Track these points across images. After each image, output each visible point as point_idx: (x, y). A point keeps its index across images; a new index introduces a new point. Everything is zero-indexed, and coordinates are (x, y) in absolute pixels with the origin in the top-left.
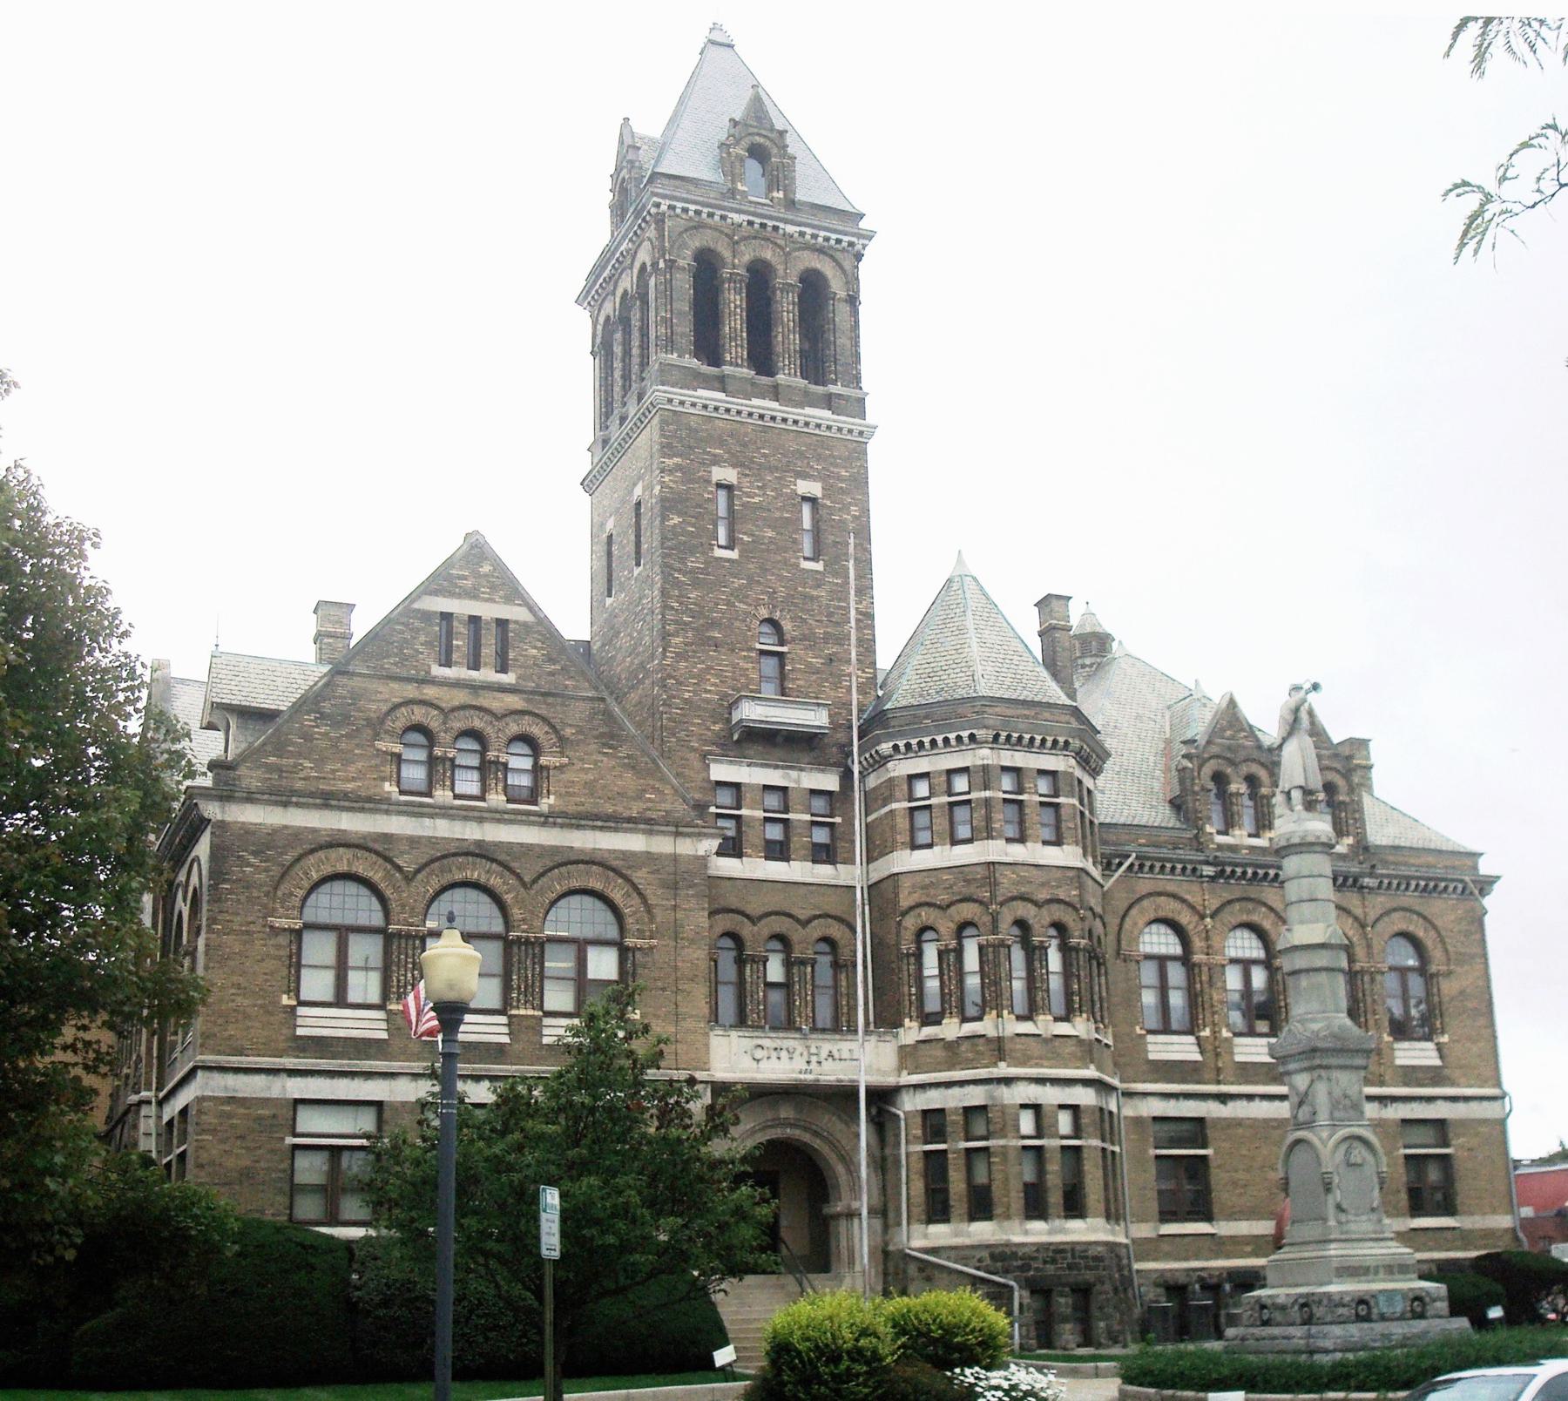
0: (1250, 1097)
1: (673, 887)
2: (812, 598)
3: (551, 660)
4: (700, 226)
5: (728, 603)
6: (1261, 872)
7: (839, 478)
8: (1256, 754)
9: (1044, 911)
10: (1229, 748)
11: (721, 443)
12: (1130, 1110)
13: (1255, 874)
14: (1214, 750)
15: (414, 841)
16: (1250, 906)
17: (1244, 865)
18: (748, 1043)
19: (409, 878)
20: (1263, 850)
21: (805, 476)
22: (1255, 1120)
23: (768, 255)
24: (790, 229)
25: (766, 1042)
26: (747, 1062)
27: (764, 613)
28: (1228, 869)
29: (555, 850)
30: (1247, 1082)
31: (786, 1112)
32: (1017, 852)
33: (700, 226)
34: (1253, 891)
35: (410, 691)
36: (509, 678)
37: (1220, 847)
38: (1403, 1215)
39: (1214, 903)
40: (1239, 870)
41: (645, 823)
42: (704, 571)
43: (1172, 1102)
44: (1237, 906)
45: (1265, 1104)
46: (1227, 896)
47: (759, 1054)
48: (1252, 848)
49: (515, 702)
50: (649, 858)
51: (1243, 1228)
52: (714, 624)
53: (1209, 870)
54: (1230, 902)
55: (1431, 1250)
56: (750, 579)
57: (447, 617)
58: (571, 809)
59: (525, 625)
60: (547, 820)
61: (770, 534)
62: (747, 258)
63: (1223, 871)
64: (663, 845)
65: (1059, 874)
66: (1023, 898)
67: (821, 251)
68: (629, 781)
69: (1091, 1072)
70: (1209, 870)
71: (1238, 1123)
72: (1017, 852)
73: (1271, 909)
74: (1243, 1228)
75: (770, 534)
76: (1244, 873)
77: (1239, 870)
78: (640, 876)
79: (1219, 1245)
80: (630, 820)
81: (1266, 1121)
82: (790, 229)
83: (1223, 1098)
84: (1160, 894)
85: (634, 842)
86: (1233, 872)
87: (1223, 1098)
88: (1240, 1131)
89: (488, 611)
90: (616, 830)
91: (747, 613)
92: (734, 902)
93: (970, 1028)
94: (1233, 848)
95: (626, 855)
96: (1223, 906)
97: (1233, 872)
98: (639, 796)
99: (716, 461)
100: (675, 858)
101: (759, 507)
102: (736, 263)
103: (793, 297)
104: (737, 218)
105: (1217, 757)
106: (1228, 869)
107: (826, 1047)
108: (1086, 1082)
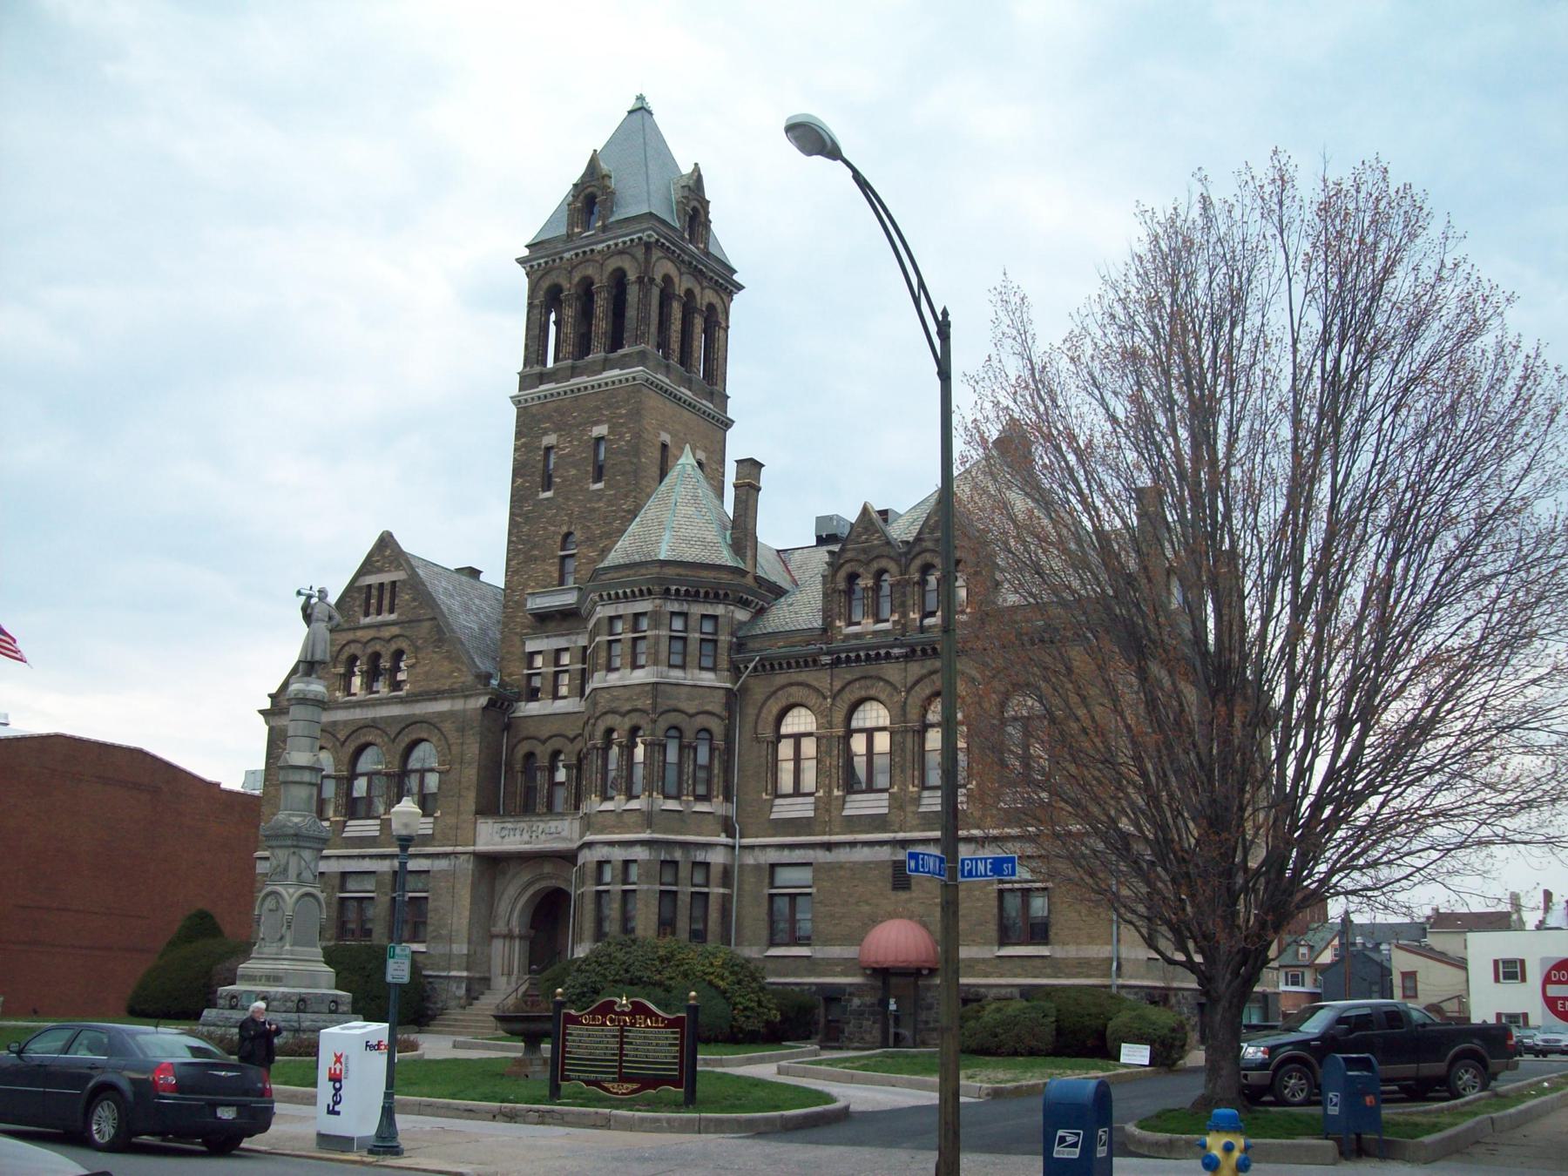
0: (853, 844)
1: (462, 730)
2: (594, 510)
3: (414, 600)
4: (551, 269)
5: (545, 529)
6: (872, 653)
7: (621, 416)
8: (886, 551)
9: (626, 719)
10: (864, 551)
11: (549, 418)
12: (749, 859)
13: (868, 655)
14: (849, 555)
15: (346, 723)
16: (869, 682)
17: (857, 650)
18: (498, 826)
19: (343, 744)
20: (886, 632)
21: (596, 423)
22: (855, 863)
23: (590, 271)
24: (600, 247)
25: (509, 825)
26: (497, 838)
27: (565, 529)
28: (843, 656)
29: (407, 717)
30: (852, 832)
31: (548, 868)
32: (613, 679)
33: (551, 269)
34: (872, 669)
35: (350, 636)
36: (393, 617)
37: (848, 637)
38: (991, 944)
39: (838, 685)
40: (853, 655)
41: (450, 693)
42: (532, 511)
43: (786, 852)
44: (857, 685)
45: (866, 850)
46: (849, 677)
47: (505, 833)
48: (875, 633)
49: (395, 630)
50: (452, 713)
51: (836, 952)
52: (533, 548)
53: (826, 659)
54: (849, 683)
55: (1015, 976)
56: (559, 508)
57: (369, 586)
58: (417, 690)
59: (403, 582)
60: (402, 701)
61: (573, 472)
62: (576, 280)
63: (839, 658)
64: (459, 705)
65: (638, 690)
66: (613, 712)
67: (621, 252)
68: (446, 667)
69: (646, 836)
70: (826, 659)
71: (841, 866)
72: (613, 679)
73: (887, 682)
74: (836, 952)
75: (573, 472)
76: (858, 656)
77: (853, 655)
78: (447, 726)
79: (810, 964)
80: (444, 692)
81: (865, 864)
82: (600, 247)
83: (828, 846)
84: (791, 684)
85: (443, 706)
86: (848, 657)
87: (828, 846)
88: (842, 873)
89: (386, 578)
90: (436, 699)
91: (554, 533)
92: (532, 731)
93: (634, 804)
94: (857, 636)
95: (441, 714)
96: (843, 688)
97: (848, 657)
98: (450, 675)
99: (545, 433)
100: (465, 711)
101: (568, 455)
102: (569, 286)
103: (604, 295)
104: (567, 255)
105: (851, 560)
106: (843, 656)
107: (542, 825)
108: (642, 843)
